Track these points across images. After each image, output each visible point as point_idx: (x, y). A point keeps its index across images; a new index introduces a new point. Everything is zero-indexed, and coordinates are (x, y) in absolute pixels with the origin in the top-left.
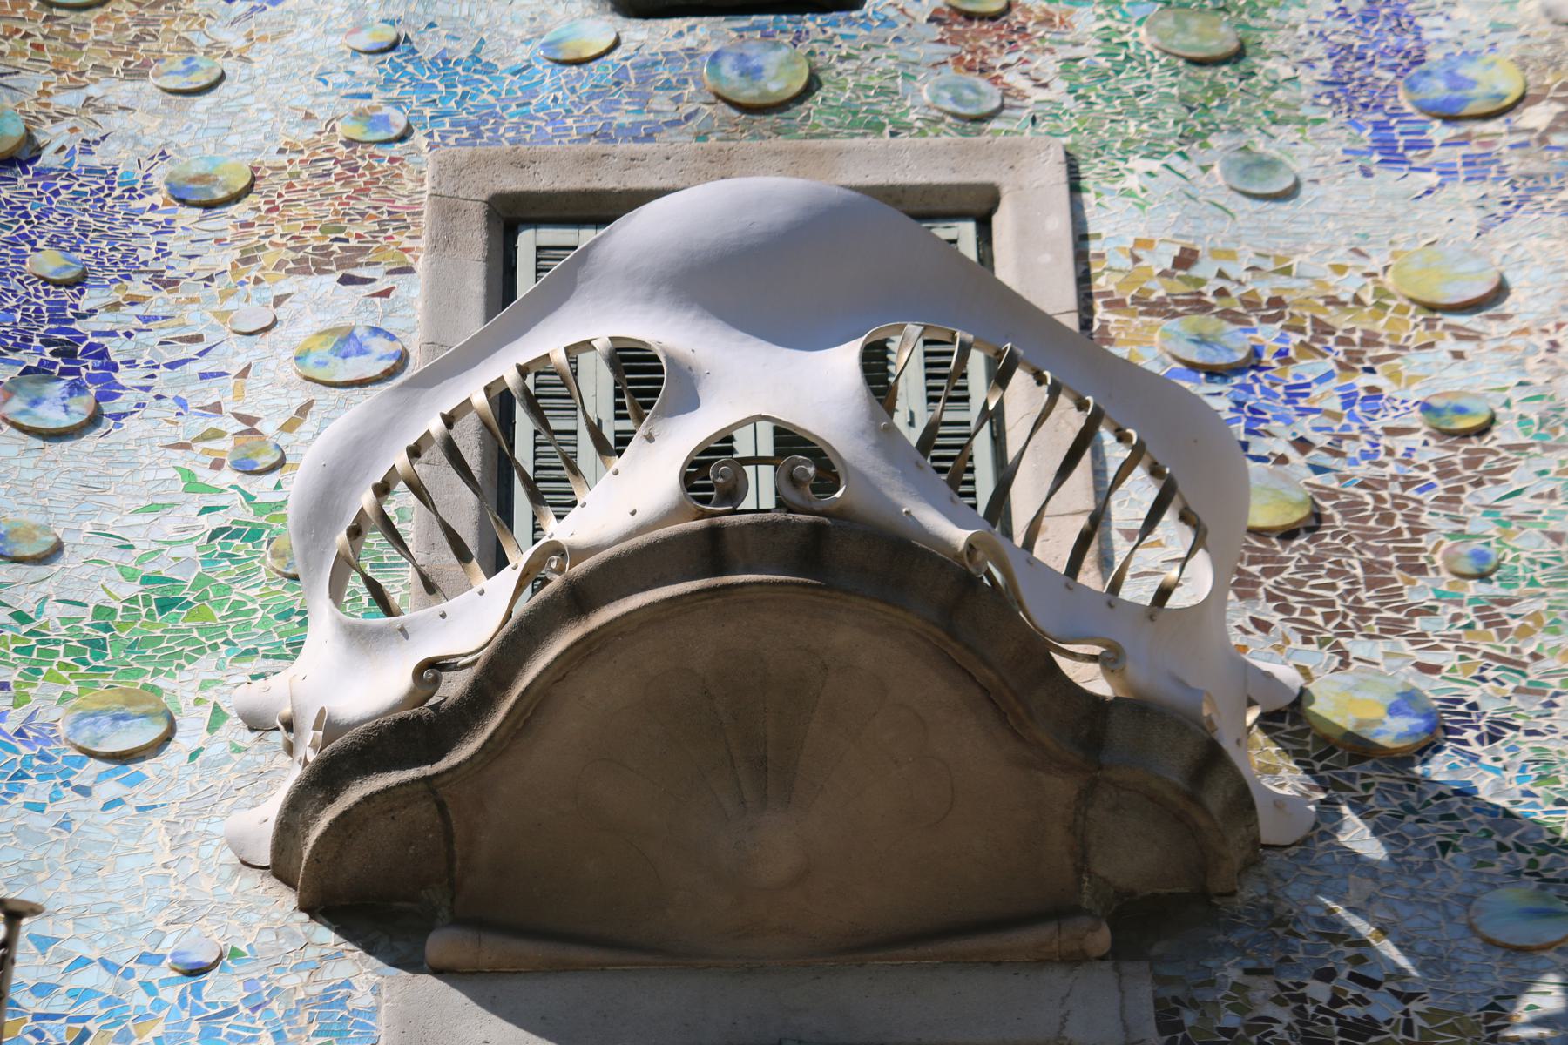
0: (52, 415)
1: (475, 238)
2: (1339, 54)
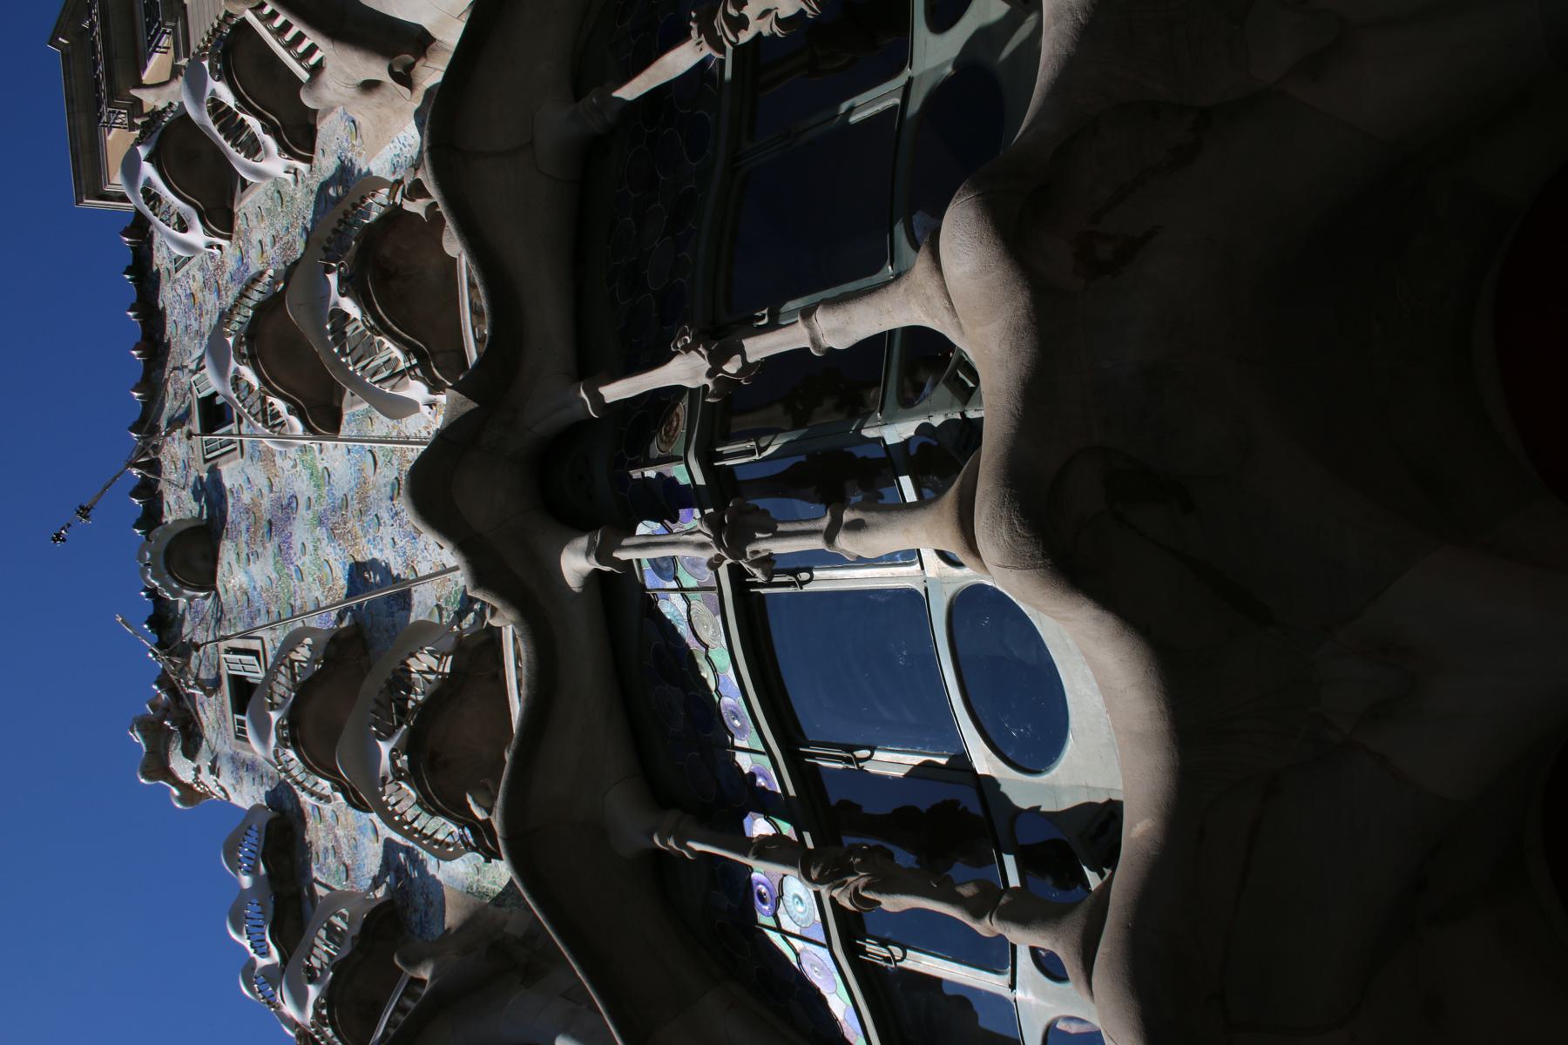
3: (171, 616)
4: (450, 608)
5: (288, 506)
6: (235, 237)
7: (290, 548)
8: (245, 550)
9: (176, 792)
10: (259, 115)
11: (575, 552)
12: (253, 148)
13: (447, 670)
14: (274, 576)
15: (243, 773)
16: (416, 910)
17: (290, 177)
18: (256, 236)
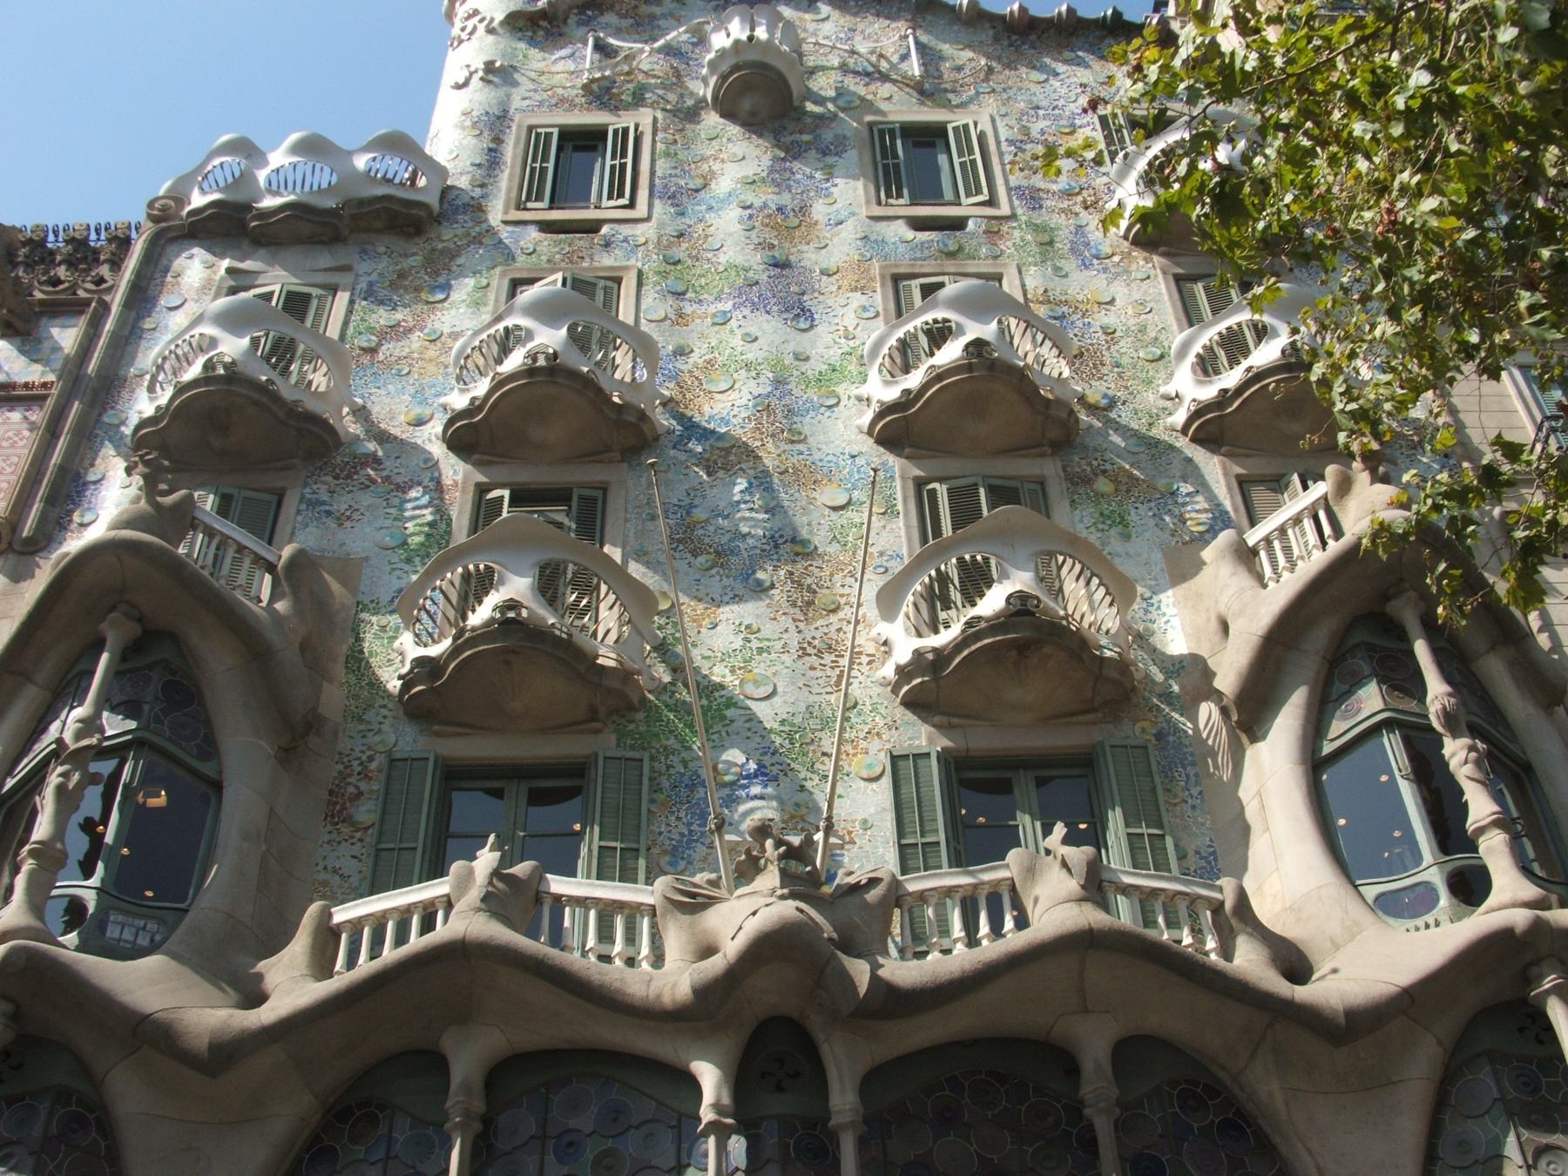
0: (803, 325)
1: (889, 284)
4: (670, 630)
5: (799, 312)
6: (1126, 244)
7: (755, 307)
8: (758, 203)
10: (1239, 390)
11: (719, 1088)
12: (1207, 366)
13: (600, 661)
14: (723, 259)
15: (486, 143)
17: (1170, 389)
18: (1119, 290)
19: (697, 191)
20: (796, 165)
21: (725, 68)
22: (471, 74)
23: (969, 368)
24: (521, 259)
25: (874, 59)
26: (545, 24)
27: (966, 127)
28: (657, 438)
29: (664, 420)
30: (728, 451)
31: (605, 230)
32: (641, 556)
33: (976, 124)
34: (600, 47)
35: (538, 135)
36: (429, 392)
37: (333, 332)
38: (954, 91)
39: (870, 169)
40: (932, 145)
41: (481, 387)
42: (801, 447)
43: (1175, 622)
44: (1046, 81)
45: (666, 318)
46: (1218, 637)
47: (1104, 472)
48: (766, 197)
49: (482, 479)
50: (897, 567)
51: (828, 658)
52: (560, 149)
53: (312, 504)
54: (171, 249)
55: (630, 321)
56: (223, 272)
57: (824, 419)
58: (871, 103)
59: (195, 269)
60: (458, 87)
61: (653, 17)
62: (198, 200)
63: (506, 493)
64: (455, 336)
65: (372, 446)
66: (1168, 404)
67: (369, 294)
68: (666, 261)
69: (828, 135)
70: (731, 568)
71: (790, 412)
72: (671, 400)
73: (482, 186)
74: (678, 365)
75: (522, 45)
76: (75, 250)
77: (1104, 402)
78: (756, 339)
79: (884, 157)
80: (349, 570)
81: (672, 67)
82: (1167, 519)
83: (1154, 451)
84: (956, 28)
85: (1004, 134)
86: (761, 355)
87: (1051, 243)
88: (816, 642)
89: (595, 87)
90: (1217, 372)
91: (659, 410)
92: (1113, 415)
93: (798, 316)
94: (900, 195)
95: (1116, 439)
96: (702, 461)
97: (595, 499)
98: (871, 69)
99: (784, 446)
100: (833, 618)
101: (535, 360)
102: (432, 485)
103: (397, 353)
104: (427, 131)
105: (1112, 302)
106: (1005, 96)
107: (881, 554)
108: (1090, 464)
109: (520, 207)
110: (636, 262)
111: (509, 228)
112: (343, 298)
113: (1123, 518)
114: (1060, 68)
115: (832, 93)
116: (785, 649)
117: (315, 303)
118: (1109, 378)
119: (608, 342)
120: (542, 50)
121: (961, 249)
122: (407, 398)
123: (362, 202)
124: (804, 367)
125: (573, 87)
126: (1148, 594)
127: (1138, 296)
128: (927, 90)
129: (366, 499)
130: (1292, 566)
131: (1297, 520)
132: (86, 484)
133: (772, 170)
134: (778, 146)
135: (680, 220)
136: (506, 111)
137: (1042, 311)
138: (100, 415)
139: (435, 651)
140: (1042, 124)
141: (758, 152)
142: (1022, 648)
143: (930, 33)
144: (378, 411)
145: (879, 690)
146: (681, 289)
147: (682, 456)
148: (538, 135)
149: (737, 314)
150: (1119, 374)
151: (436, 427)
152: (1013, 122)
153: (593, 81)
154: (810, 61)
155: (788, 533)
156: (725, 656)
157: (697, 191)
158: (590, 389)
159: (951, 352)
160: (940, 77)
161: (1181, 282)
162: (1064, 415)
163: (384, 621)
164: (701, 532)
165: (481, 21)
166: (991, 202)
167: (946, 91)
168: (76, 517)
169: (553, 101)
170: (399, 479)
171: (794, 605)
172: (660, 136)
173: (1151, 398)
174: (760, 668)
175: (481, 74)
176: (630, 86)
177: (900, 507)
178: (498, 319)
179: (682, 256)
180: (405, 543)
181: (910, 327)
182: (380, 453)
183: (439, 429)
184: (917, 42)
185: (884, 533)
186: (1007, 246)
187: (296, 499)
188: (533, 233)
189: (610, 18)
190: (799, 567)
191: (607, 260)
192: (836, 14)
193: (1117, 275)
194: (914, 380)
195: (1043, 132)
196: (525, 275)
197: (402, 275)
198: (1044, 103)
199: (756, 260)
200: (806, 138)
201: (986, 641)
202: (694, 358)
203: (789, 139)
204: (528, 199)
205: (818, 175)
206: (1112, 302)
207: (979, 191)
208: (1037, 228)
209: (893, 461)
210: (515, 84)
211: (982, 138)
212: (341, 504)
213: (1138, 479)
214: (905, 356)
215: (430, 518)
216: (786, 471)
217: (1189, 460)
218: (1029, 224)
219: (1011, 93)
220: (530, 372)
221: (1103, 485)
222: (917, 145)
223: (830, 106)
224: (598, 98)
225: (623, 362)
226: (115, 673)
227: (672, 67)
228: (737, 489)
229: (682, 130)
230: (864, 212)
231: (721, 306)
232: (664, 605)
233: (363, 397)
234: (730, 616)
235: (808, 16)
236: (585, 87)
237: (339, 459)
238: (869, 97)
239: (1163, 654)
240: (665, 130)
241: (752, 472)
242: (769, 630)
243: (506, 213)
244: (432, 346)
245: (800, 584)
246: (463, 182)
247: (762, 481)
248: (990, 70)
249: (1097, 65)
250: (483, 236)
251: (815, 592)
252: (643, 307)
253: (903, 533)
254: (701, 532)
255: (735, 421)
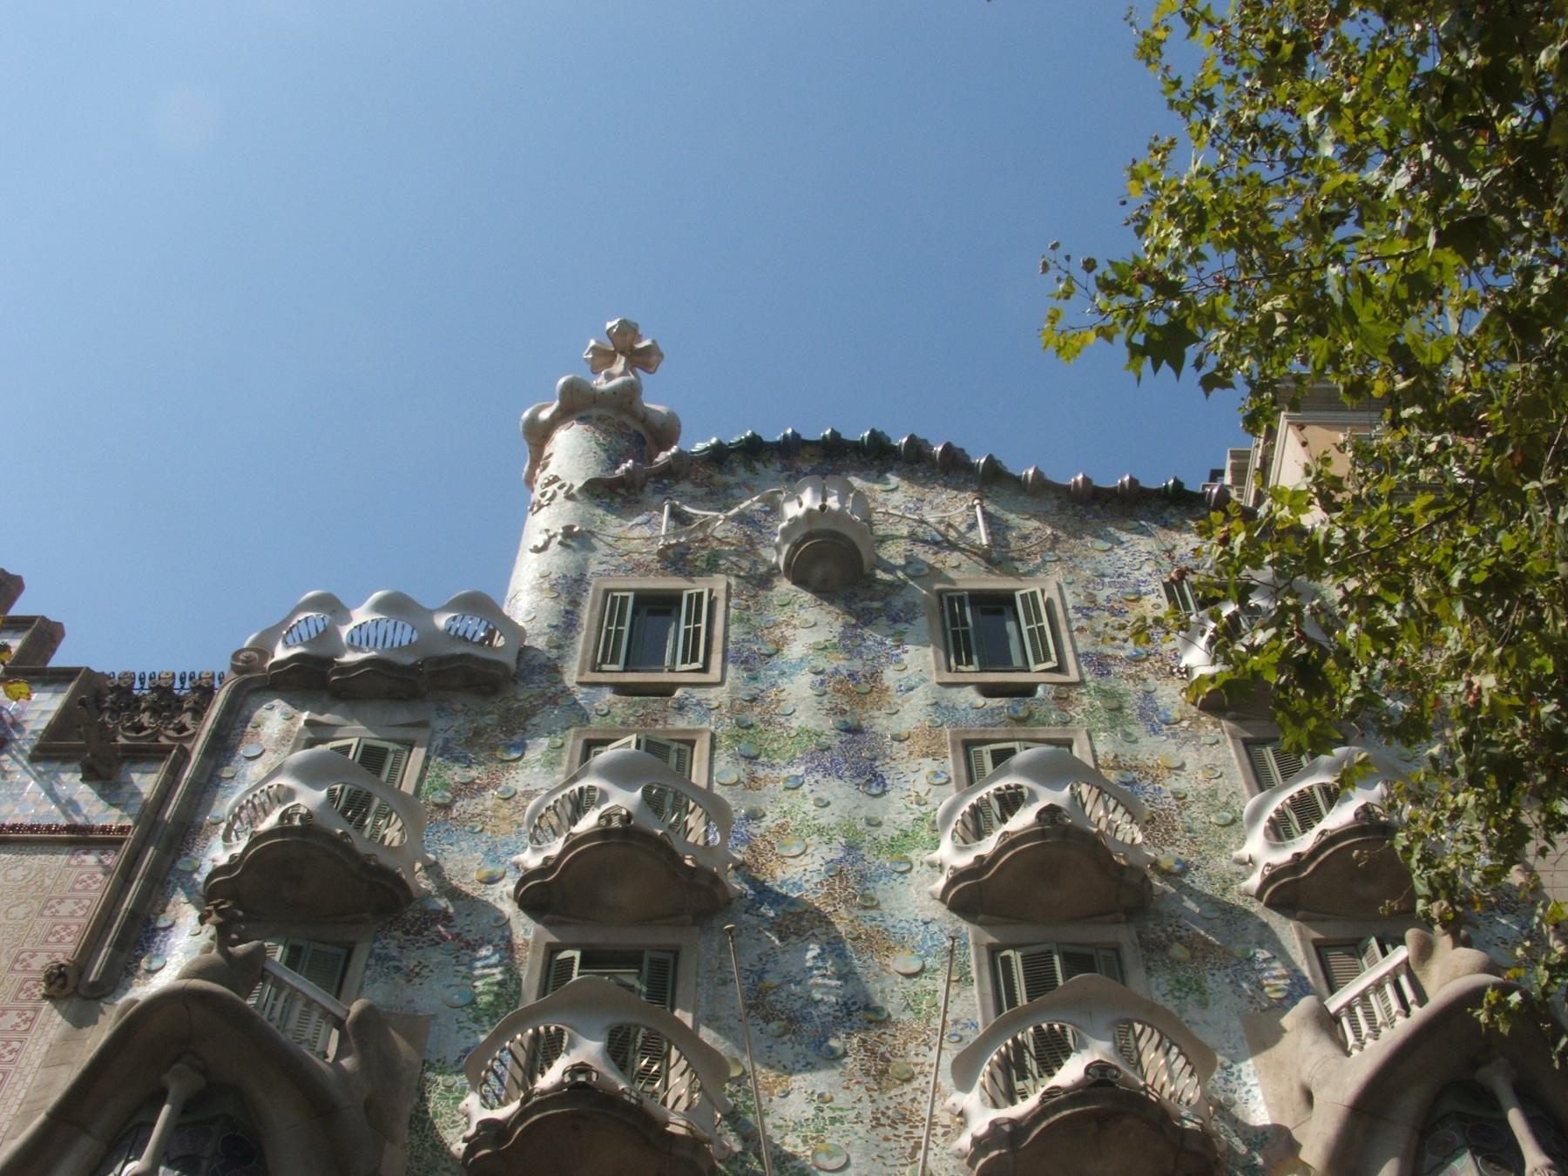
0: (875, 791)
1: (960, 750)
2: (1141, 708)
3: (759, 466)
4: (741, 1098)
6: (1194, 709)
7: (827, 772)
8: (829, 668)
9: (545, 415)
12: (1279, 831)
13: (670, 1128)
14: (795, 723)
16: (401, 948)
18: (1189, 755)
19: (770, 656)
20: (867, 632)
21: (797, 536)
22: (550, 538)
23: (1042, 834)
24: (596, 720)
25: (942, 528)
26: (622, 491)
27: (1033, 594)
28: (729, 902)
29: (737, 885)
30: (800, 916)
31: (679, 693)
32: (711, 1020)
33: (1043, 592)
34: (676, 515)
35: (614, 598)
36: (501, 850)
37: (408, 787)
38: (1020, 560)
39: (940, 637)
40: (1000, 612)
41: (555, 847)
42: (874, 913)
43: (1257, 1091)
44: (1111, 549)
45: (738, 782)
46: (1301, 1107)
47: (1179, 938)
48: (837, 662)
49: (553, 939)
50: (972, 1036)
51: (902, 1129)
52: (635, 612)
53: (382, 959)
54: (253, 700)
55: (703, 784)
56: (302, 723)
57: (896, 884)
58: (940, 571)
59: (275, 720)
60: (537, 550)
61: (726, 486)
62: (281, 653)
63: (577, 954)
64: (529, 795)
65: (443, 903)
66: (1242, 869)
67: (448, 752)
68: (739, 724)
69: (898, 603)
70: (802, 1035)
71: (863, 878)
72: (743, 864)
73: (559, 647)
74: (750, 828)
75: (600, 512)
76: (160, 698)
77: (1177, 867)
78: (828, 804)
79: (954, 624)
80: (416, 1027)
81: (745, 534)
82: (1245, 985)
83: (1229, 916)
84: (1021, 498)
85: (1071, 601)
86: (833, 820)
87: (1120, 709)
88: (890, 1112)
89: (670, 552)
90: (1290, 836)
91: (731, 874)
92: (1186, 880)
93: (870, 781)
94: (969, 662)
95: (1190, 905)
96: (775, 926)
97: (666, 962)
98: (939, 538)
99: (856, 912)
100: (907, 1088)
101: (609, 821)
102: (502, 944)
103: (470, 810)
104: (505, 593)
105: (1182, 767)
106: (1071, 564)
107: (956, 1022)
108: (1164, 931)
109: (595, 668)
110: (709, 725)
111: (585, 690)
112: (419, 754)
113: (1200, 986)
114: (1124, 537)
115: (902, 562)
116: (859, 1119)
117: (391, 758)
118: (1181, 843)
119: (680, 807)
120: (619, 516)
121: (1031, 715)
122: (479, 855)
123: (440, 660)
124: (876, 832)
125: (648, 553)
126: (1228, 1063)
127: (1208, 761)
128: (996, 558)
129: (436, 956)
130: (1376, 1032)
131: (1378, 986)
132: (156, 930)
133: (843, 637)
134: (850, 614)
135: (753, 685)
136: (583, 575)
137: (1112, 776)
138: (174, 861)
139: (501, 1113)
140: (1108, 591)
141: (829, 618)
142: (1101, 1119)
143: (996, 503)
144: (449, 867)
145: (955, 1162)
146: (754, 752)
147: (754, 921)
148: (614, 598)
149: (810, 779)
150: (1191, 839)
151: (508, 885)
152: (1080, 590)
153: (668, 547)
154: (881, 530)
155: (861, 999)
156: (798, 1125)
157: (770, 656)
158: (664, 851)
159: (1023, 819)
160: (1007, 546)
161: (1250, 747)
162: (1137, 880)
163: (450, 1081)
164: (773, 998)
165: (561, 487)
166: (1061, 668)
167: (1013, 559)
168: (144, 963)
169: (629, 566)
170: (469, 937)
171: (867, 1073)
172: (733, 601)
173: (1225, 862)
174: (832, 1139)
175: (559, 538)
176: (704, 552)
177: (974, 975)
178: (574, 780)
179: (754, 720)
180: (474, 1002)
181: (982, 793)
182: (451, 910)
183: (512, 887)
184: (984, 513)
185: (958, 1001)
186: (1076, 712)
187: (367, 953)
188: (608, 695)
189: (686, 487)
190: (873, 1035)
191: (680, 723)
192: (904, 485)
193: (1186, 740)
194: (988, 846)
195: (1109, 600)
196: (599, 736)
197: (477, 733)
198: (1110, 571)
199: (828, 725)
200: (876, 604)
201: (1065, 1113)
202: (767, 822)
203: (861, 605)
204: (604, 661)
205: (889, 642)
206: (1182, 767)
207: (1047, 658)
208: (1105, 694)
209: (967, 929)
210: (593, 549)
211: (1049, 605)
212: (410, 961)
213: (1213, 945)
214: (977, 824)
215: (499, 977)
216: (859, 937)
217: (1265, 926)
218: (1098, 690)
219: (1077, 561)
220: (603, 833)
221: (1178, 951)
222: (985, 612)
223: (900, 574)
224: (673, 563)
225: (696, 824)
226: (173, 1128)
227: (745, 534)
228: (810, 955)
229: (755, 596)
230: (934, 679)
231: (794, 771)
232: (735, 1072)
233: (435, 853)
234: (802, 1084)
235: (877, 487)
236: (660, 553)
237: (410, 914)
238: (938, 565)
239: (1245, 1125)
240: (738, 596)
241: (824, 938)
242: (842, 1099)
243: (581, 674)
244: (505, 804)
245: (873, 1053)
246: (540, 643)
247: (834, 947)
248: (1056, 539)
249: (1161, 533)
250: (558, 697)
251: (888, 1061)
252: (716, 770)
253: (977, 1000)
254: (773, 998)
255: (807, 886)
